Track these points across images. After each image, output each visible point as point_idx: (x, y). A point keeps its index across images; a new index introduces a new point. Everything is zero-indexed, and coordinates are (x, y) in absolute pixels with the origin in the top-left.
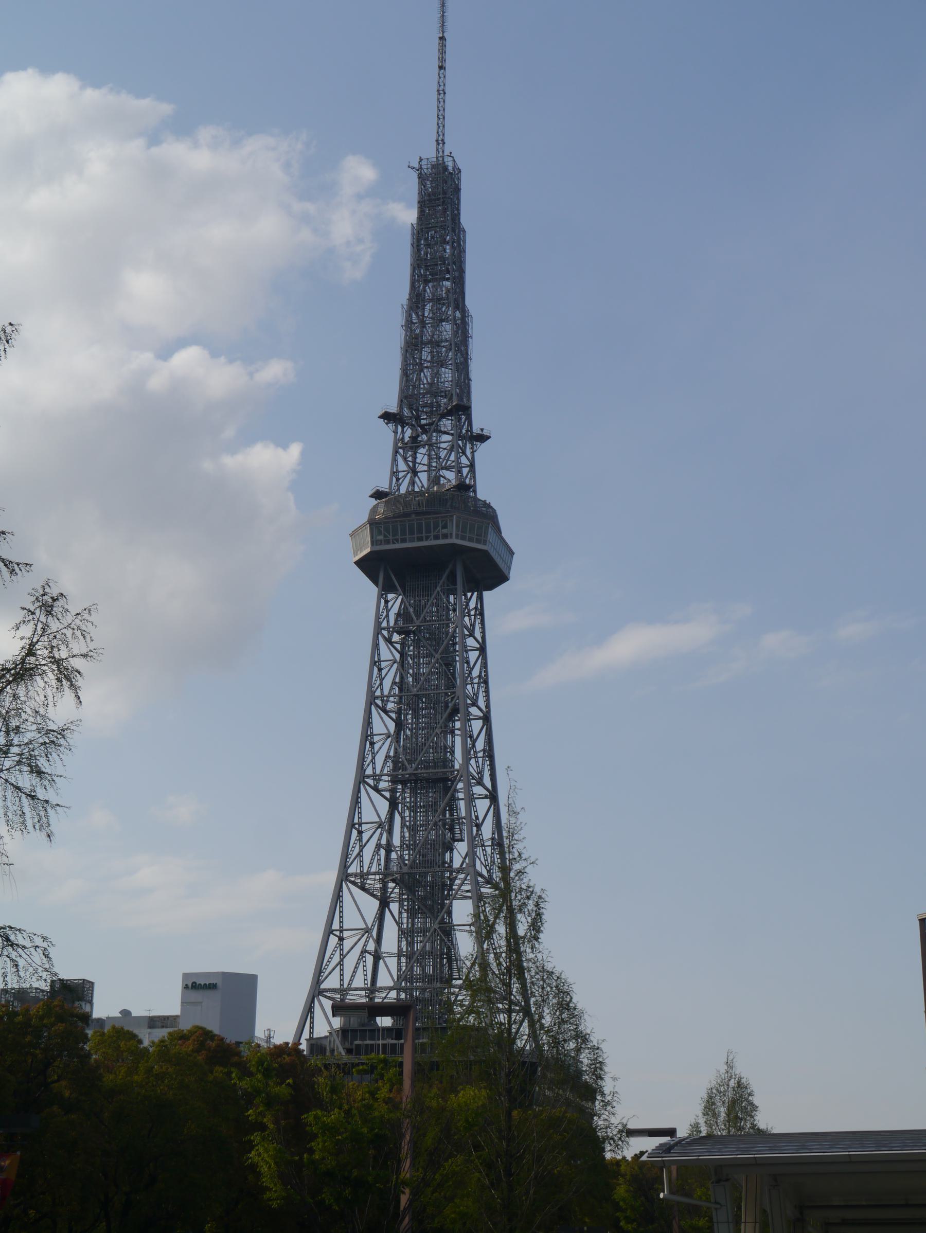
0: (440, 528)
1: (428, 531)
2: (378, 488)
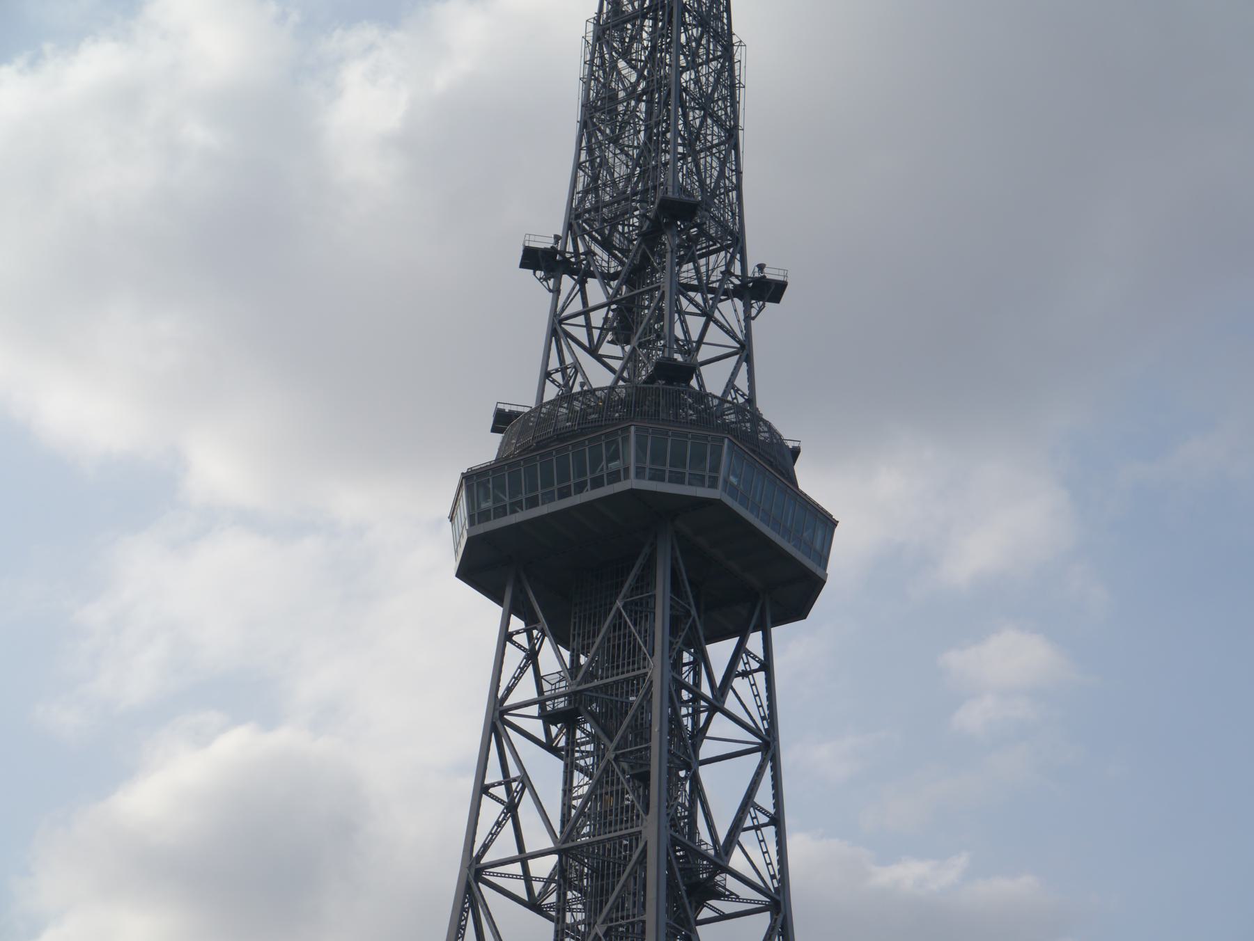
0: (604, 463)
1: (581, 472)
2: (500, 406)
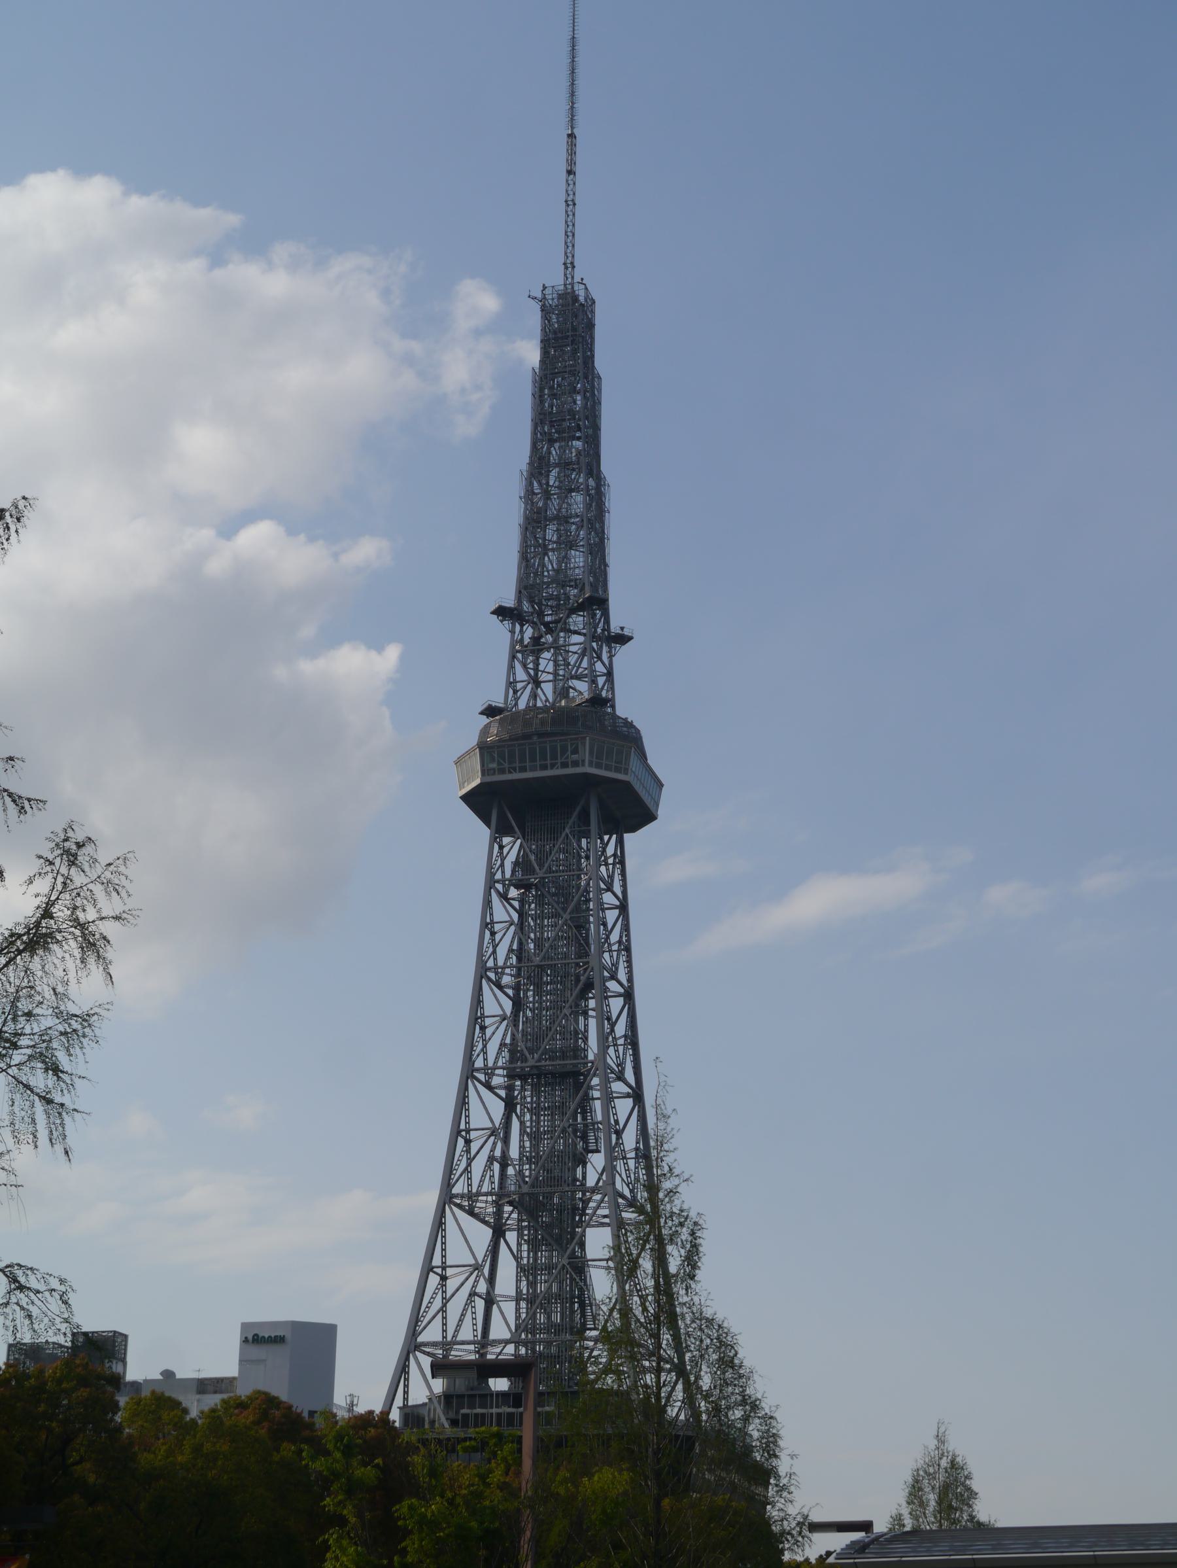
0: (569, 753)
1: (554, 757)
2: (490, 703)
